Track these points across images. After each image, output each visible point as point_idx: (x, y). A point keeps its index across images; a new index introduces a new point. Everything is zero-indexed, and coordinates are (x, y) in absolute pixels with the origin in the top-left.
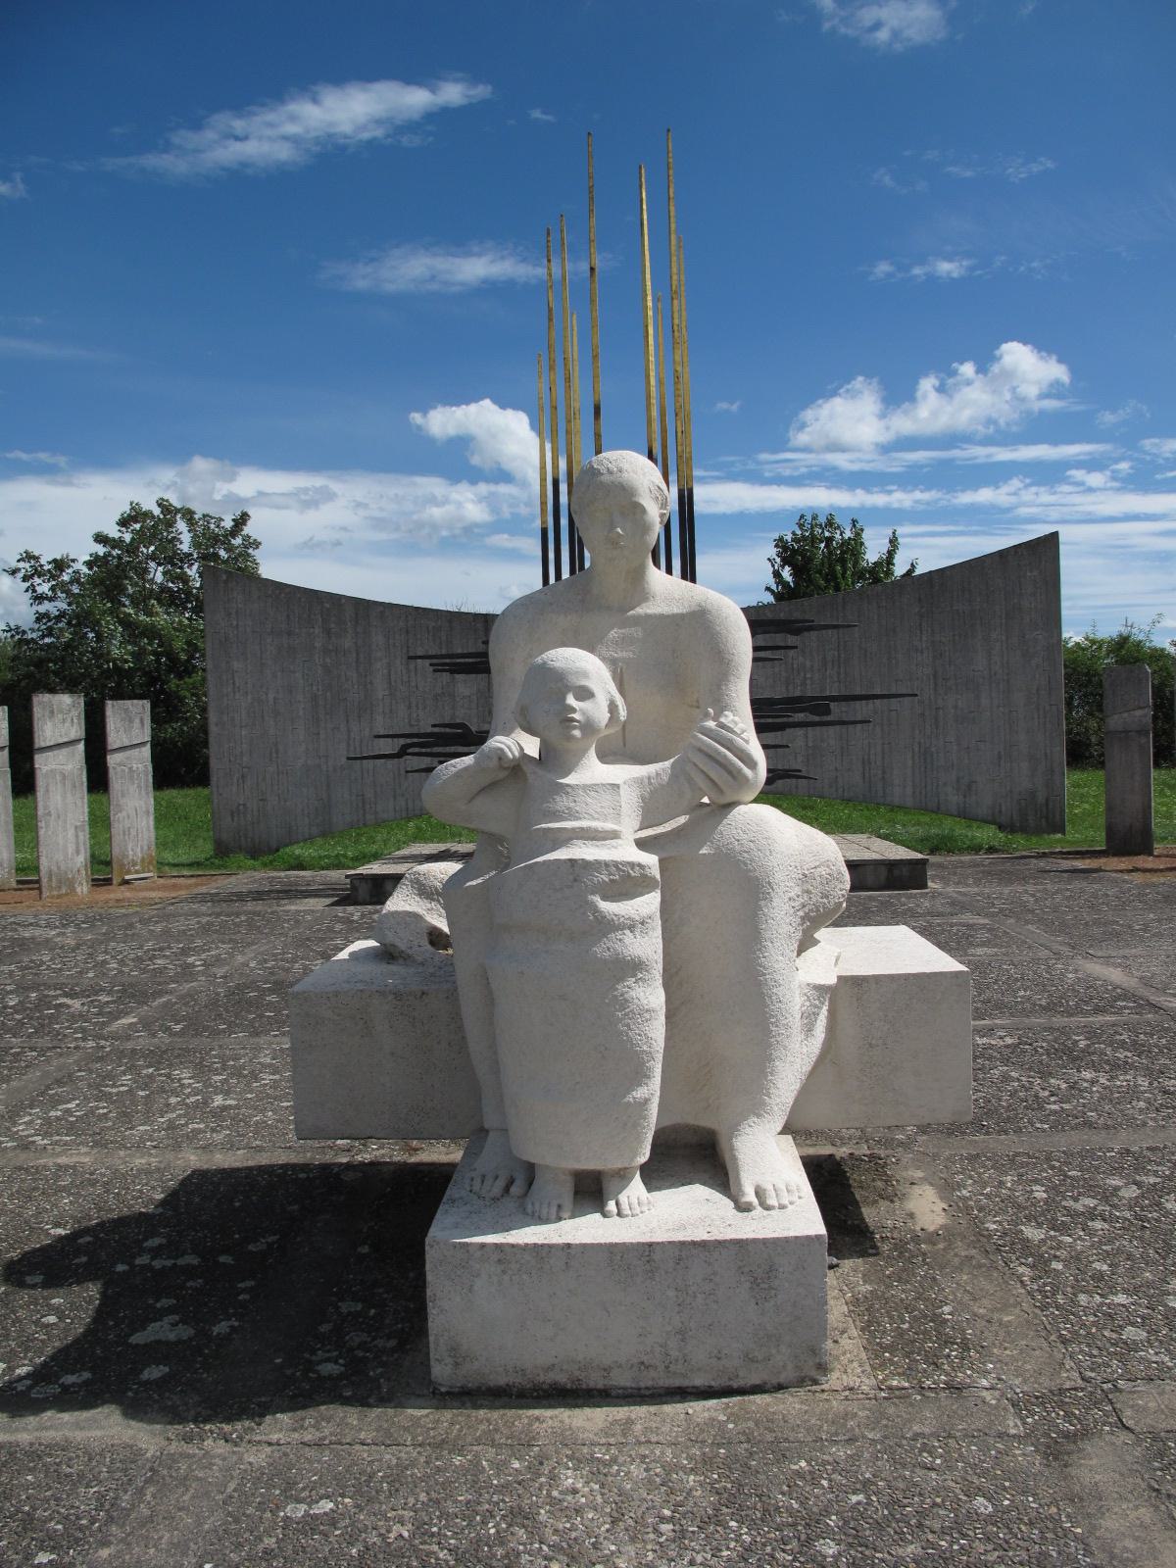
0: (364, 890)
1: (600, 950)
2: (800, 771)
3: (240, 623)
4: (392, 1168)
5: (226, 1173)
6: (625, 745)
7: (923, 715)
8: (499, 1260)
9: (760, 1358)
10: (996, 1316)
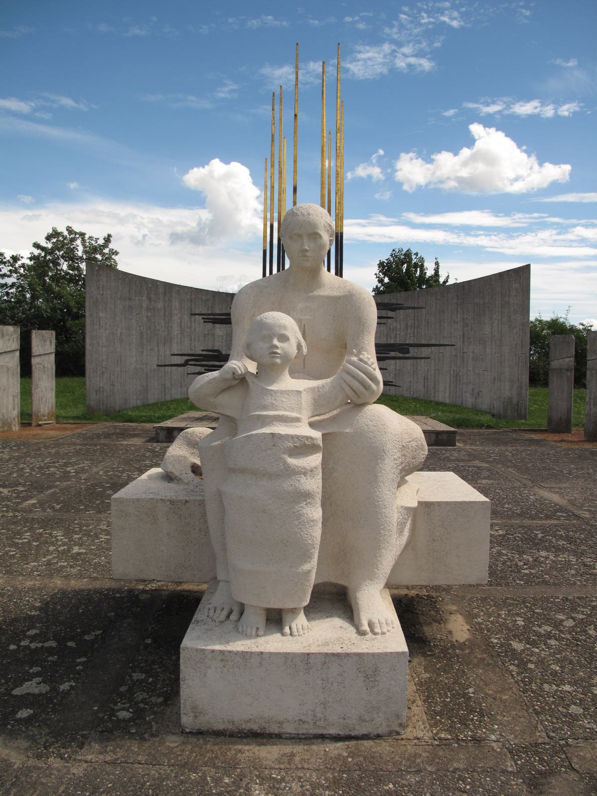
0: (162, 435)
1: (287, 485)
2: (392, 382)
3: (105, 293)
4: (167, 593)
5: (77, 593)
6: (304, 367)
8: (222, 660)
9: (368, 720)
10: (498, 695)
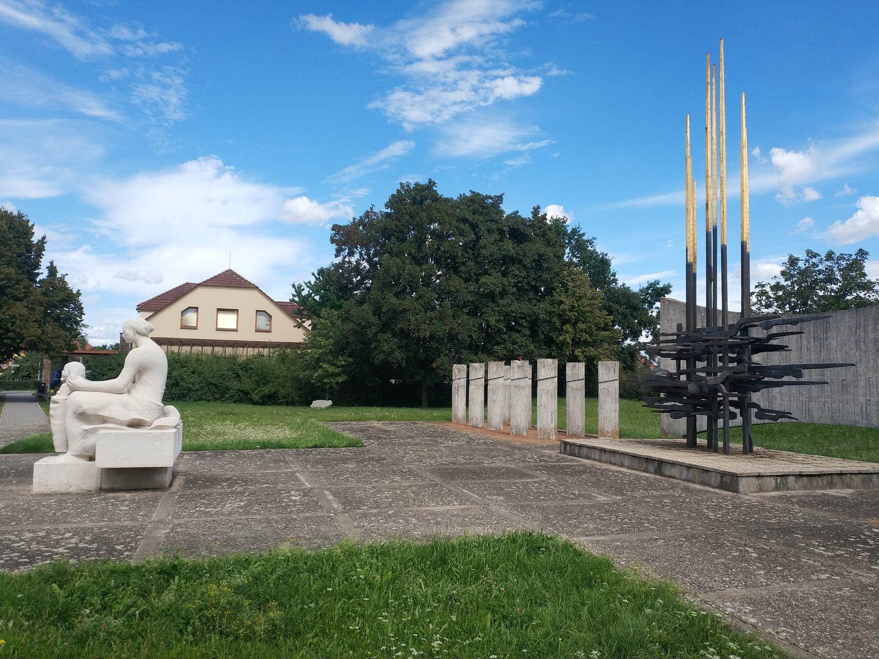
2: (791, 414)
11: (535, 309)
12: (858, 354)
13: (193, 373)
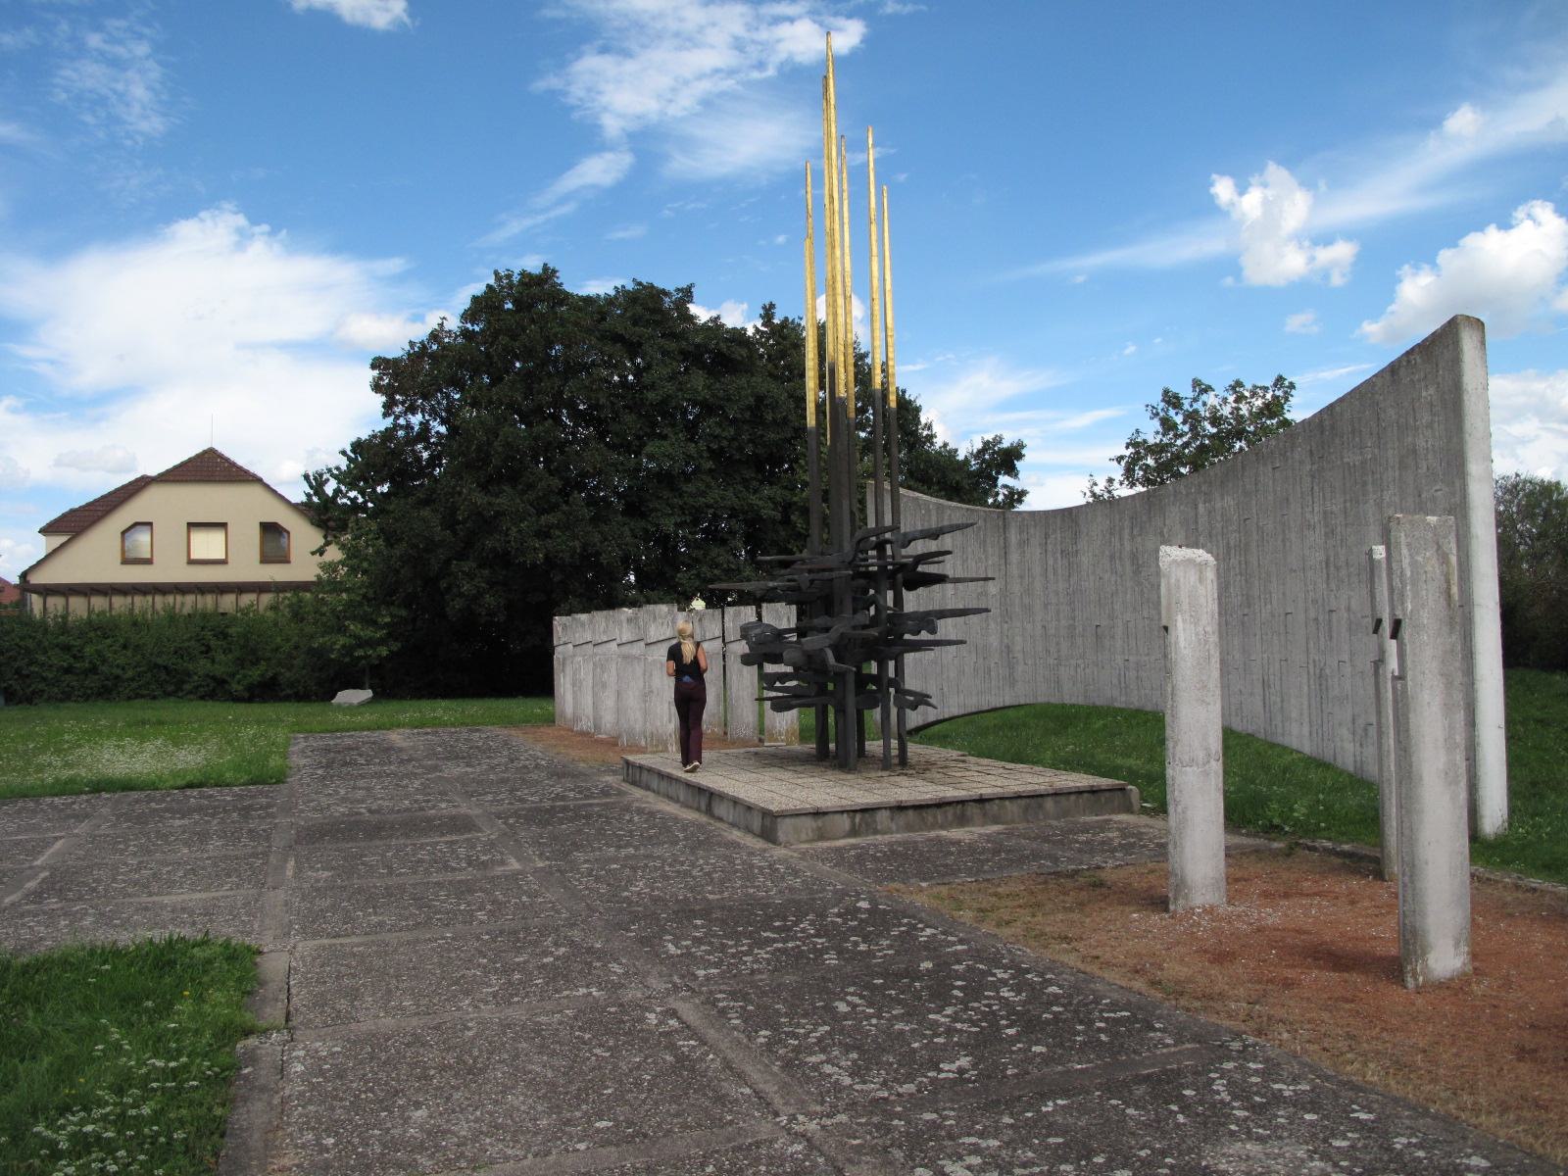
7: (1316, 619)
11: (753, 499)
12: (1113, 579)
13: (125, 647)
